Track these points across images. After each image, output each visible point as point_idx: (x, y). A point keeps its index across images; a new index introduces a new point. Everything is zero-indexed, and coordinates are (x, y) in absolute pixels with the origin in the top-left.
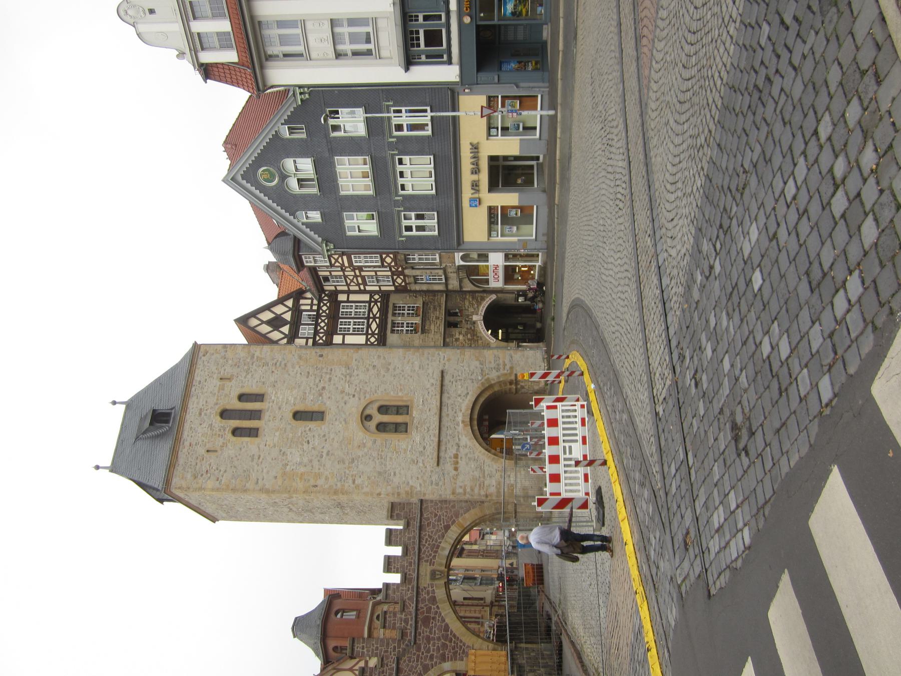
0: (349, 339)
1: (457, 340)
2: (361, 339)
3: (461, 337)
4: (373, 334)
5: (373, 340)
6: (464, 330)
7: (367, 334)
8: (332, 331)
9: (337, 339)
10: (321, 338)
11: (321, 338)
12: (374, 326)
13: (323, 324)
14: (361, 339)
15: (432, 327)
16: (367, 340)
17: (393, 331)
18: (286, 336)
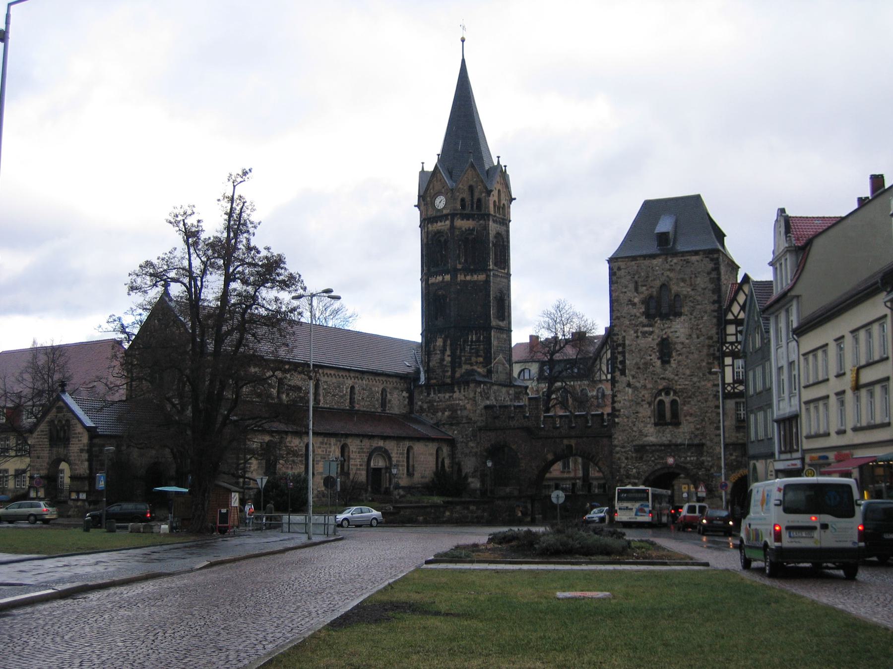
0: (728, 371)
1: (731, 455)
2: (729, 379)
3: (734, 457)
4: (734, 388)
5: (729, 388)
6: (739, 459)
7: (735, 382)
8: (735, 355)
9: (728, 361)
10: (727, 348)
11: (727, 348)
12: (741, 388)
13: (739, 347)
14: (729, 379)
15: (742, 434)
16: (729, 384)
17: (737, 403)
18: (736, 317)
